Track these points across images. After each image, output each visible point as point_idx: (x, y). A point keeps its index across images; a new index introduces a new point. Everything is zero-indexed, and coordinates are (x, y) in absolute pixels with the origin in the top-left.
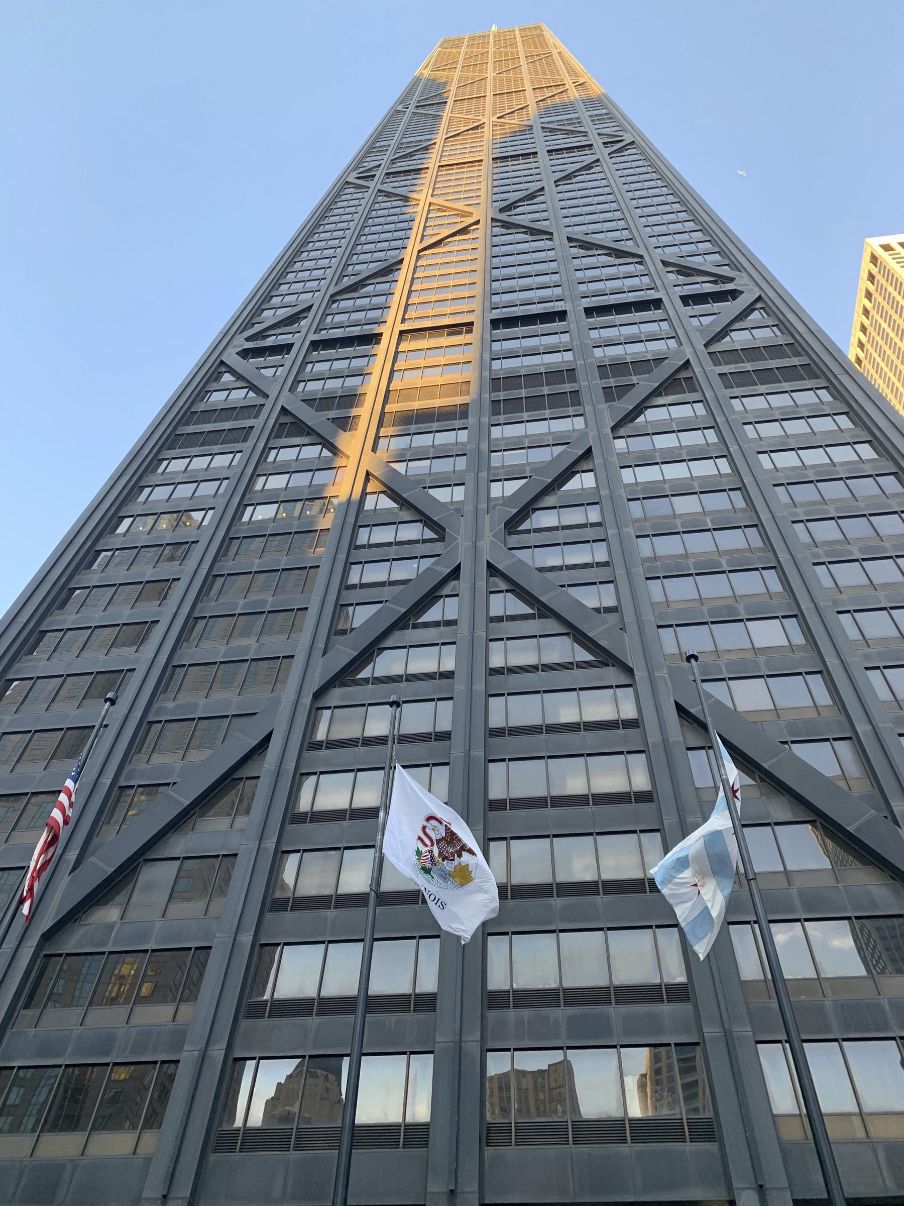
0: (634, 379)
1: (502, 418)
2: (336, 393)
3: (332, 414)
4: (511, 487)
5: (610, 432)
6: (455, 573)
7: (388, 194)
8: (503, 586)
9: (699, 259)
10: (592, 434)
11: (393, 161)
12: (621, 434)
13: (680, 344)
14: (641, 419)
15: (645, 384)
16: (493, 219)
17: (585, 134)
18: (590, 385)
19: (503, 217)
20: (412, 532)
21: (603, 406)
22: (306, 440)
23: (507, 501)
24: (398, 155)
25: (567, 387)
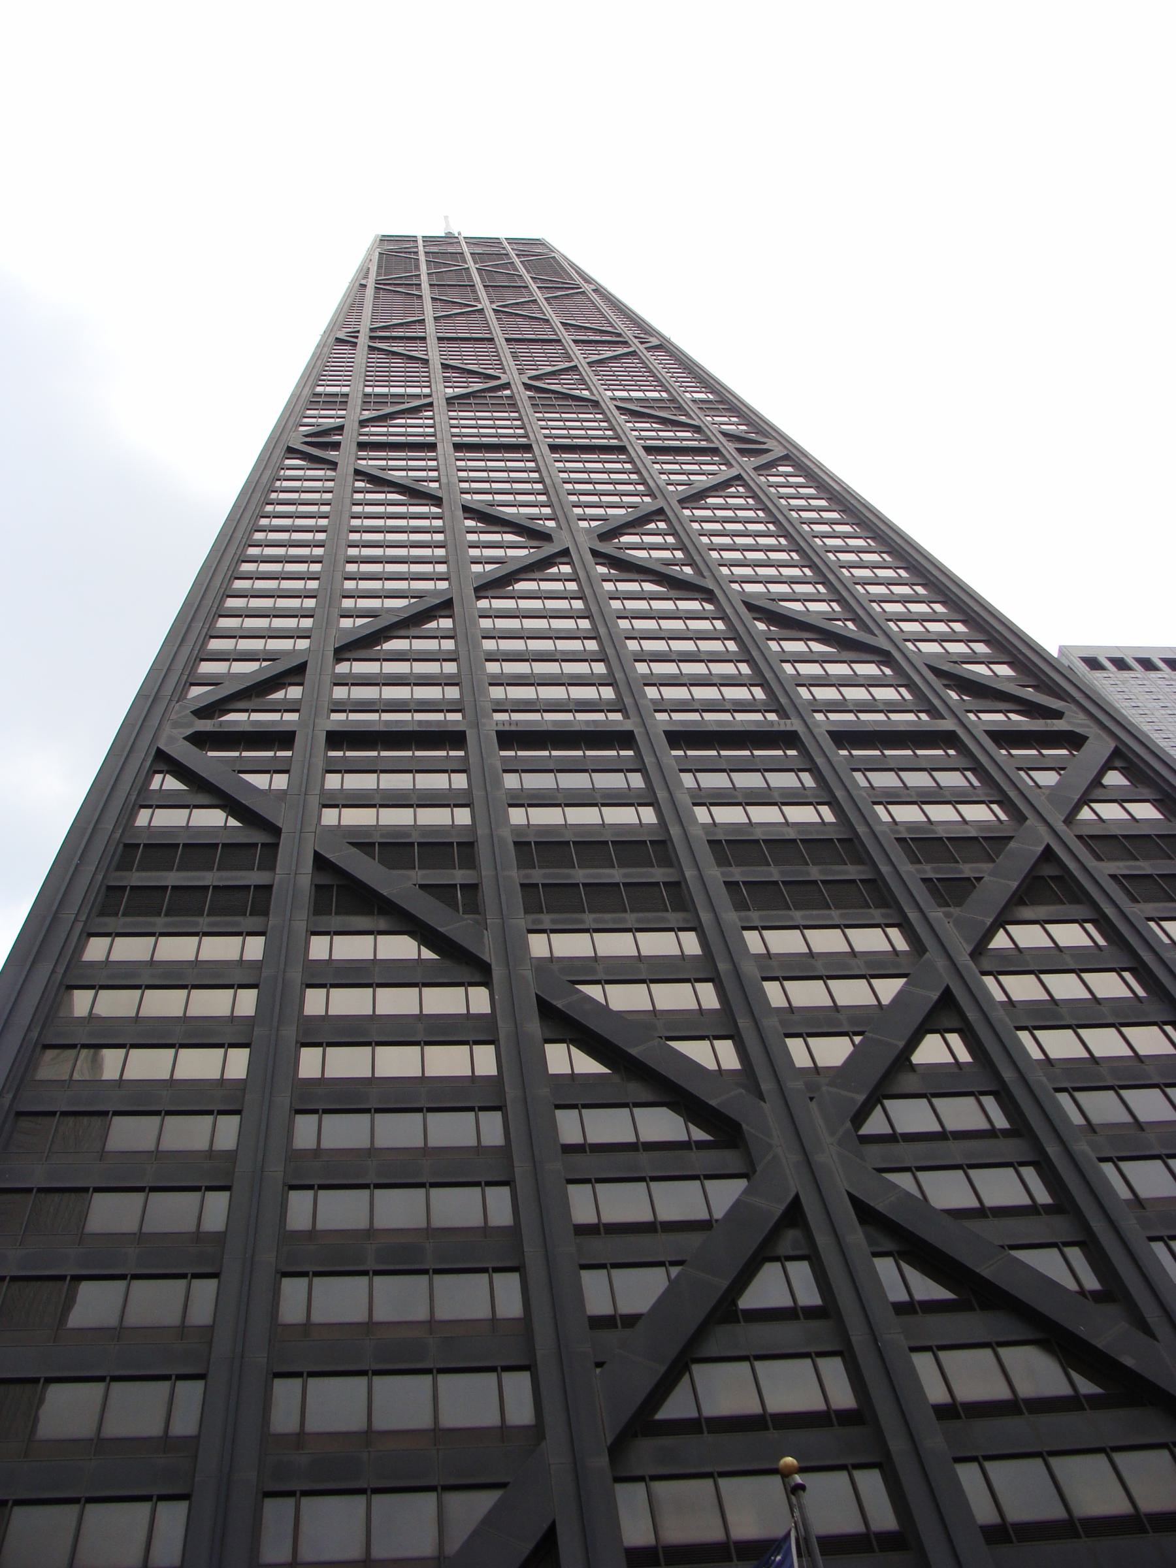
0: (967, 870)
1: (755, 916)
2: (410, 836)
3: (419, 876)
4: (834, 1052)
5: (971, 963)
6: (794, 1214)
7: (378, 482)
8: (889, 1245)
9: (981, 669)
10: (941, 963)
11: (363, 423)
12: (987, 968)
13: (1017, 816)
14: (1000, 941)
15: (997, 881)
16: (595, 553)
17: (697, 429)
18: (912, 873)
19: (606, 548)
20: (662, 1125)
21: (936, 914)
22: (382, 924)
23: (839, 1074)
24: (367, 414)
25: (852, 872)
